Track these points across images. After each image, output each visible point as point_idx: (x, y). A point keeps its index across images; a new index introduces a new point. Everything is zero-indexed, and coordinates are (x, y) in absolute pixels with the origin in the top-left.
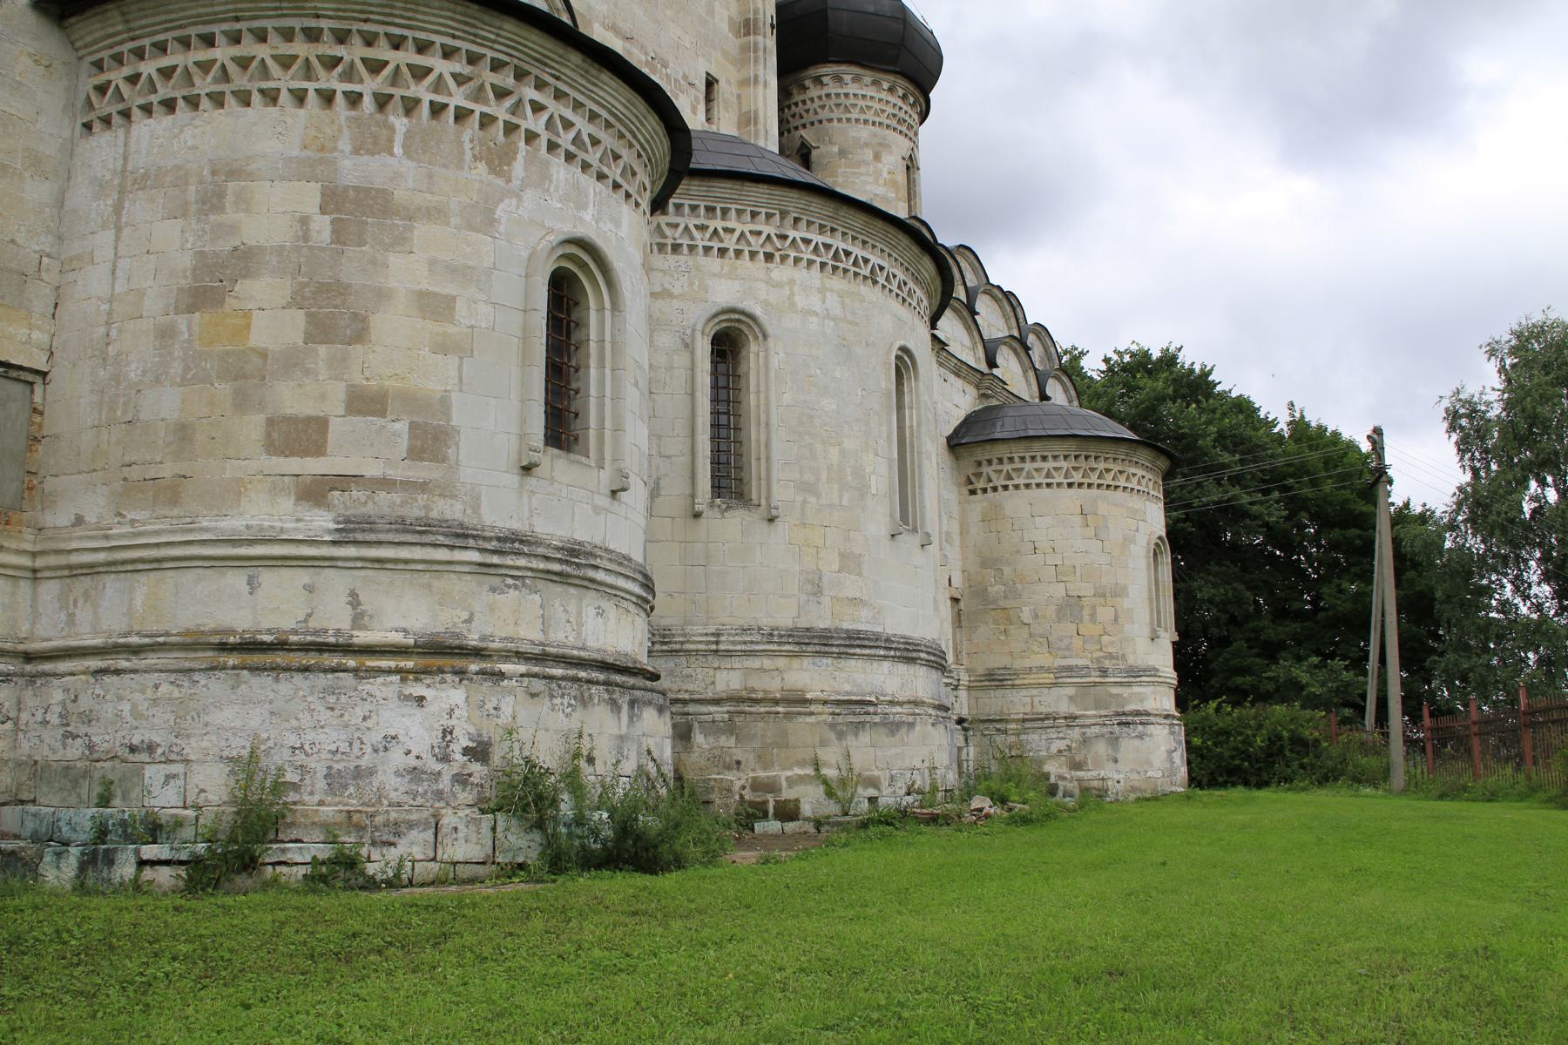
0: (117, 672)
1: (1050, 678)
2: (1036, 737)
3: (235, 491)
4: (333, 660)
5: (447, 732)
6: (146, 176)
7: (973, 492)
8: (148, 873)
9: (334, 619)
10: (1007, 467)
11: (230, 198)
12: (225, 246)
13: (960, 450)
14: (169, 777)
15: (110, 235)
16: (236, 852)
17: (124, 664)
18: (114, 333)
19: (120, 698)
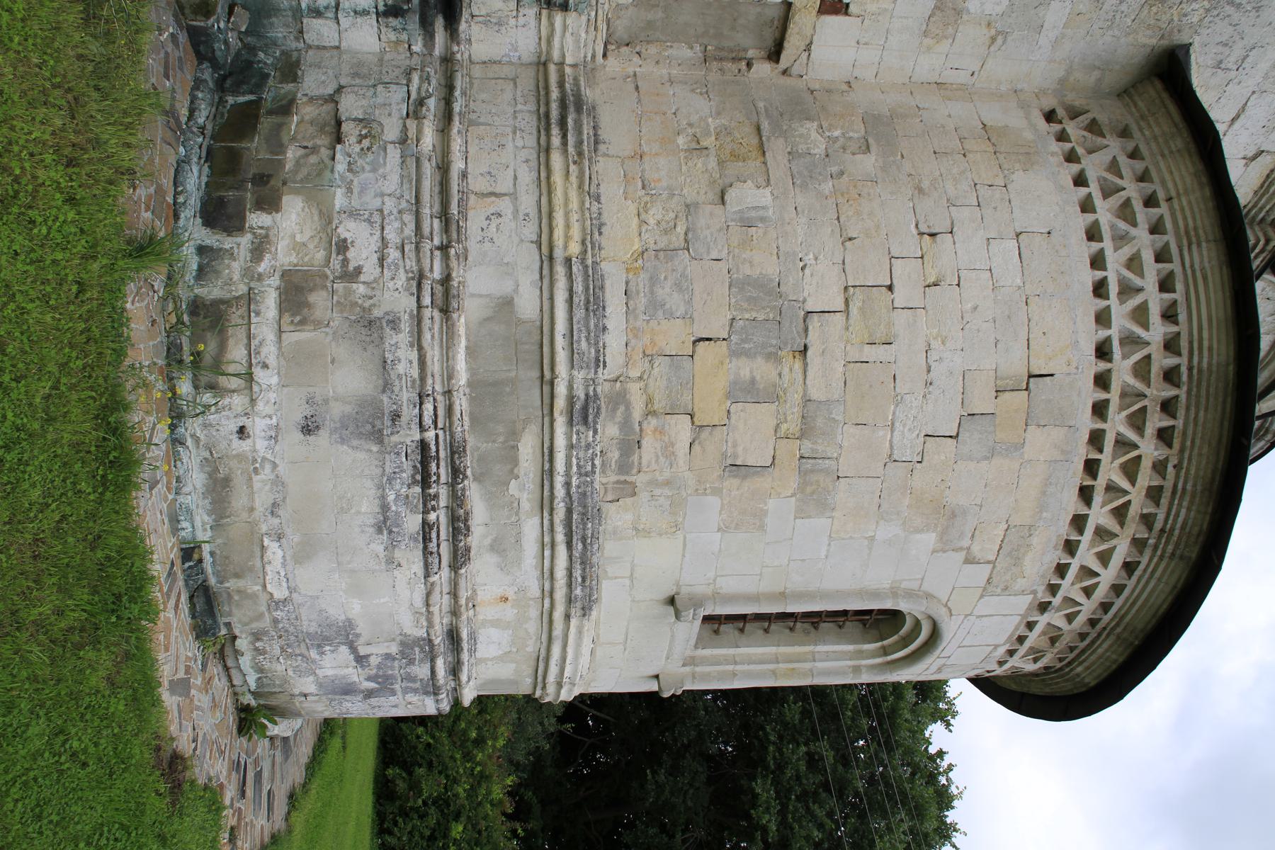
1: (568, 243)
2: (392, 182)
7: (1050, 116)
10: (1132, 190)
13: (1155, 90)
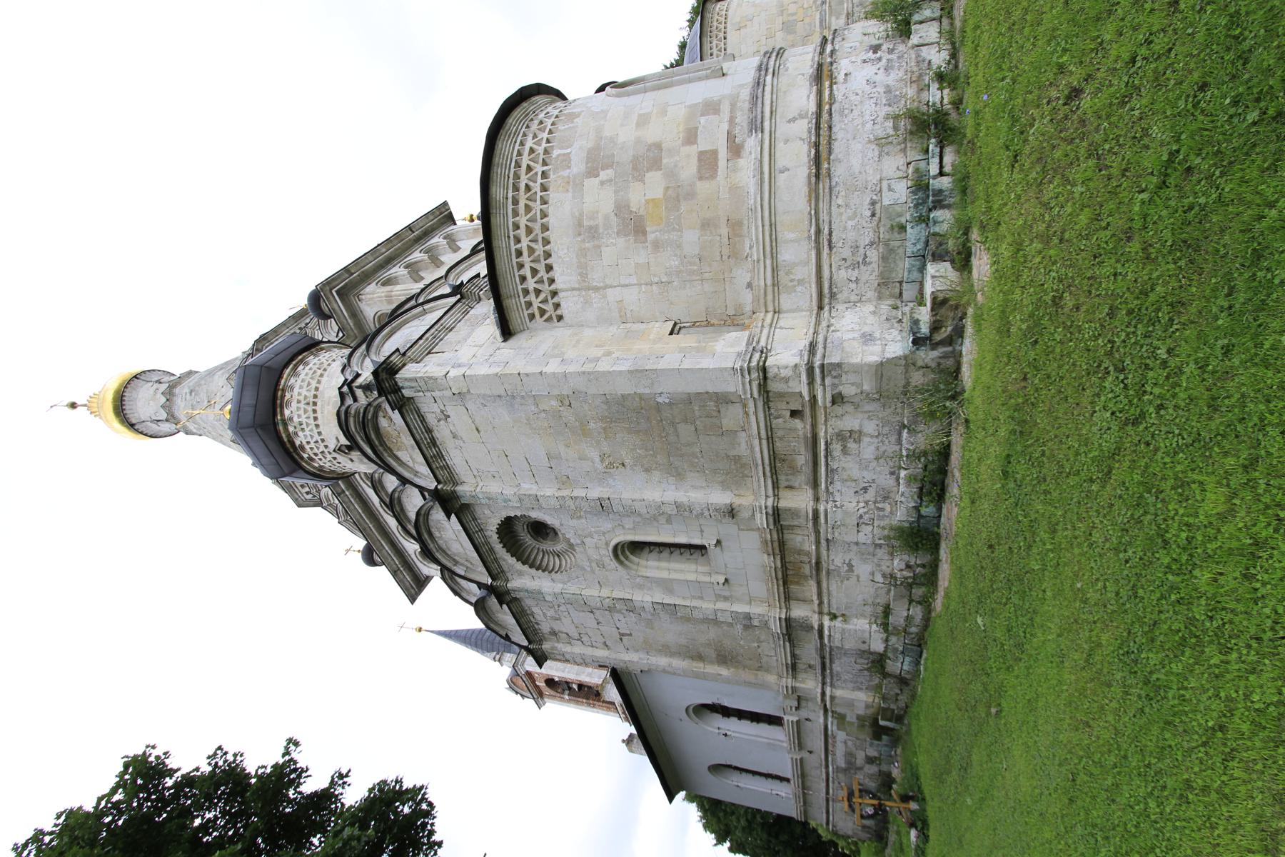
0: (830, 234)
3: (735, 190)
4: (824, 126)
5: (865, 61)
6: (581, 274)
8: (947, 169)
9: (804, 127)
11: (592, 223)
12: (614, 220)
14: (890, 189)
15: (609, 291)
16: (931, 127)
17: (826, 231)
18: (656, 280)
19: (845, 228)
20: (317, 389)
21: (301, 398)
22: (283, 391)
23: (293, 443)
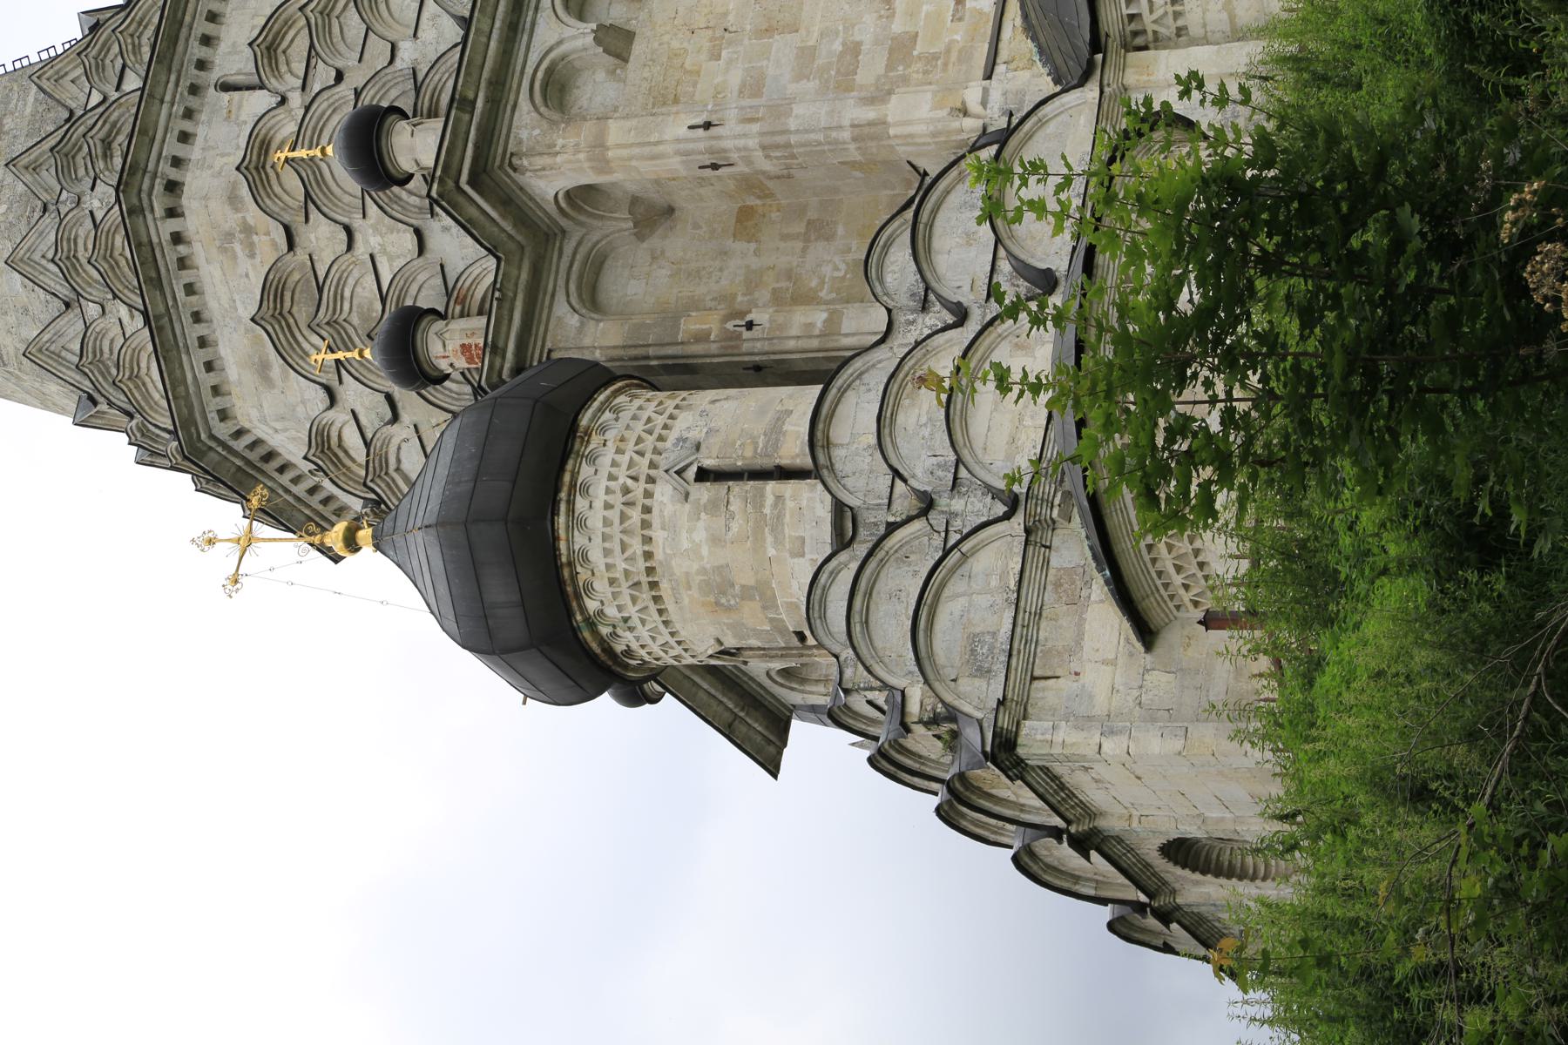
20: (648, 555)
21: (619, 574)
22: (570, 564)
23: (609, 651)
